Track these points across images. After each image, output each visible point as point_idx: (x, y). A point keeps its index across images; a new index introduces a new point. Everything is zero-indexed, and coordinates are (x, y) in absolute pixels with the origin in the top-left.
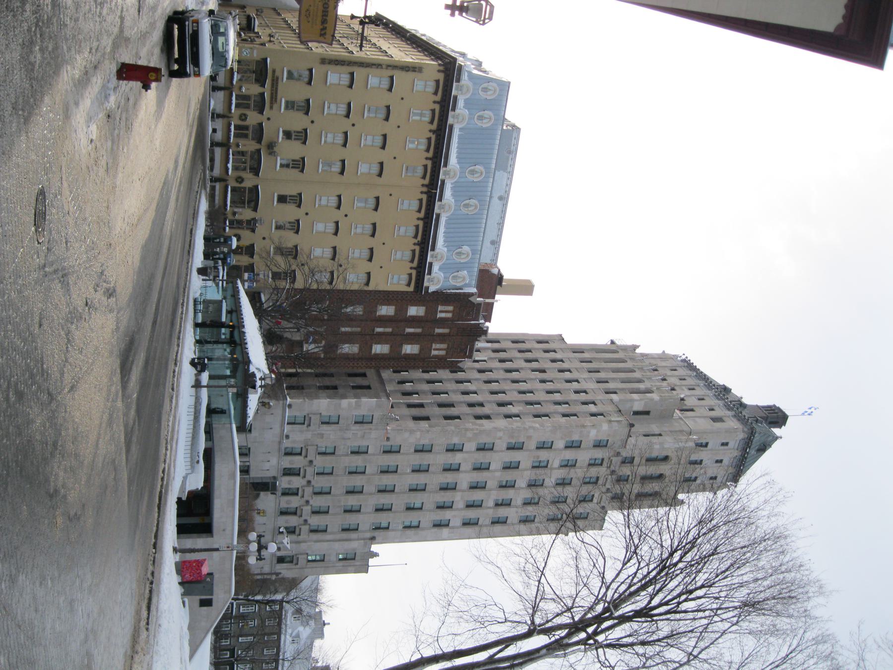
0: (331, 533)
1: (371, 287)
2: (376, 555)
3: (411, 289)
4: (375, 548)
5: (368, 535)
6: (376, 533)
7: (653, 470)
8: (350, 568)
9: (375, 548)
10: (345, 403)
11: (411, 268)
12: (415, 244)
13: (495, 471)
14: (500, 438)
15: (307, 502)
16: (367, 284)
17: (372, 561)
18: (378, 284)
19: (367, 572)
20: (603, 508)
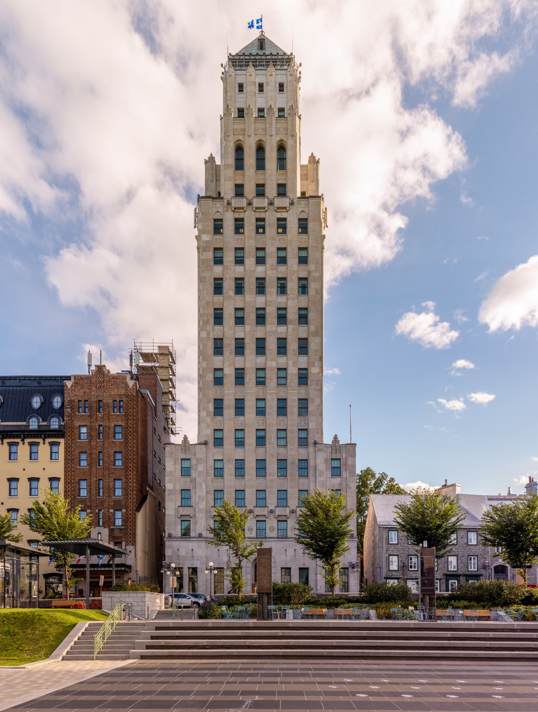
0: (309, 486)
1: (61, 474)
2: (336, 437)
3: (62, 441)
4: (327, 440)
5: (311, 449)
6: (311, 441)
7: (250, 159)
8: (350, 463)
9: (327, 440)
10: (169, 486)
11: (44, 444)
12: (24, 444)
13: (245, 331)
14: (208, 334)
15: (272, 512)
16: (58, 479)
17: (343, 440)
18: (58, 469)
19: (355, 445)
20: (292, 204)
